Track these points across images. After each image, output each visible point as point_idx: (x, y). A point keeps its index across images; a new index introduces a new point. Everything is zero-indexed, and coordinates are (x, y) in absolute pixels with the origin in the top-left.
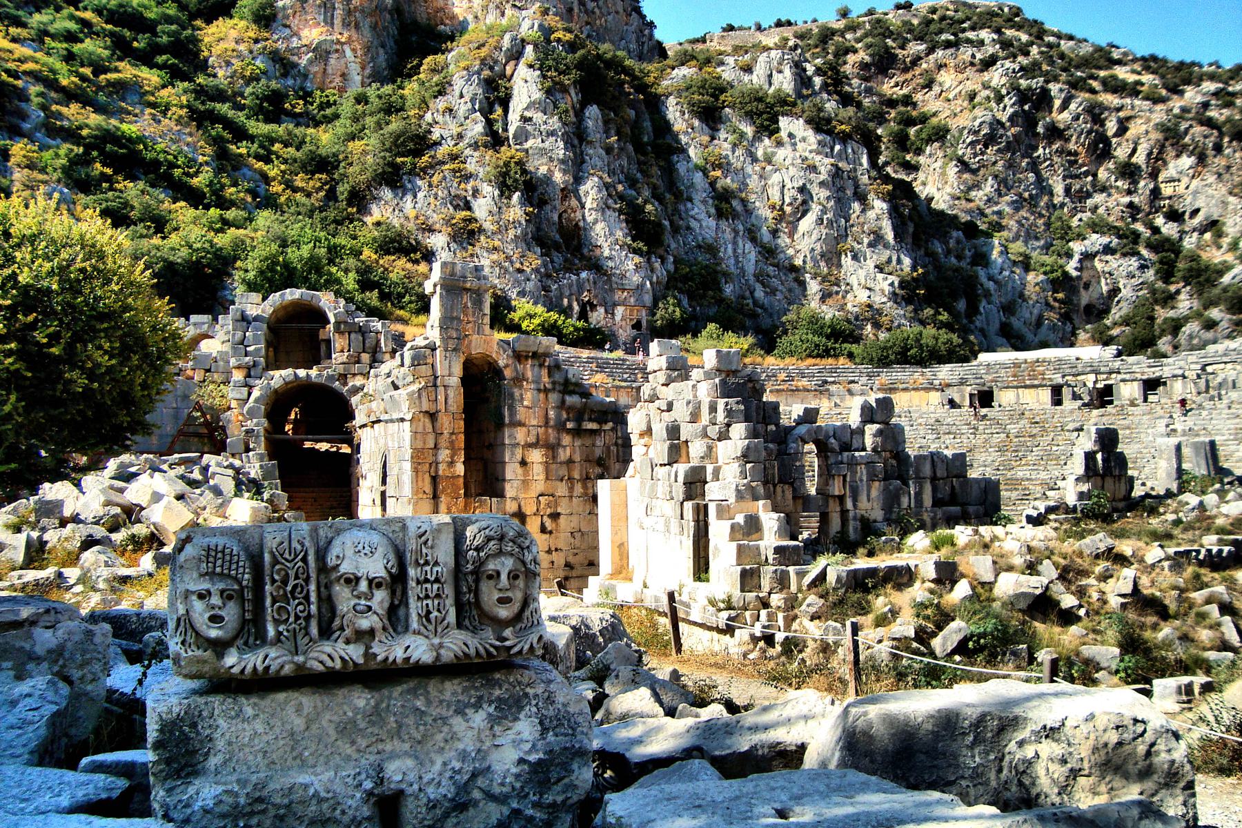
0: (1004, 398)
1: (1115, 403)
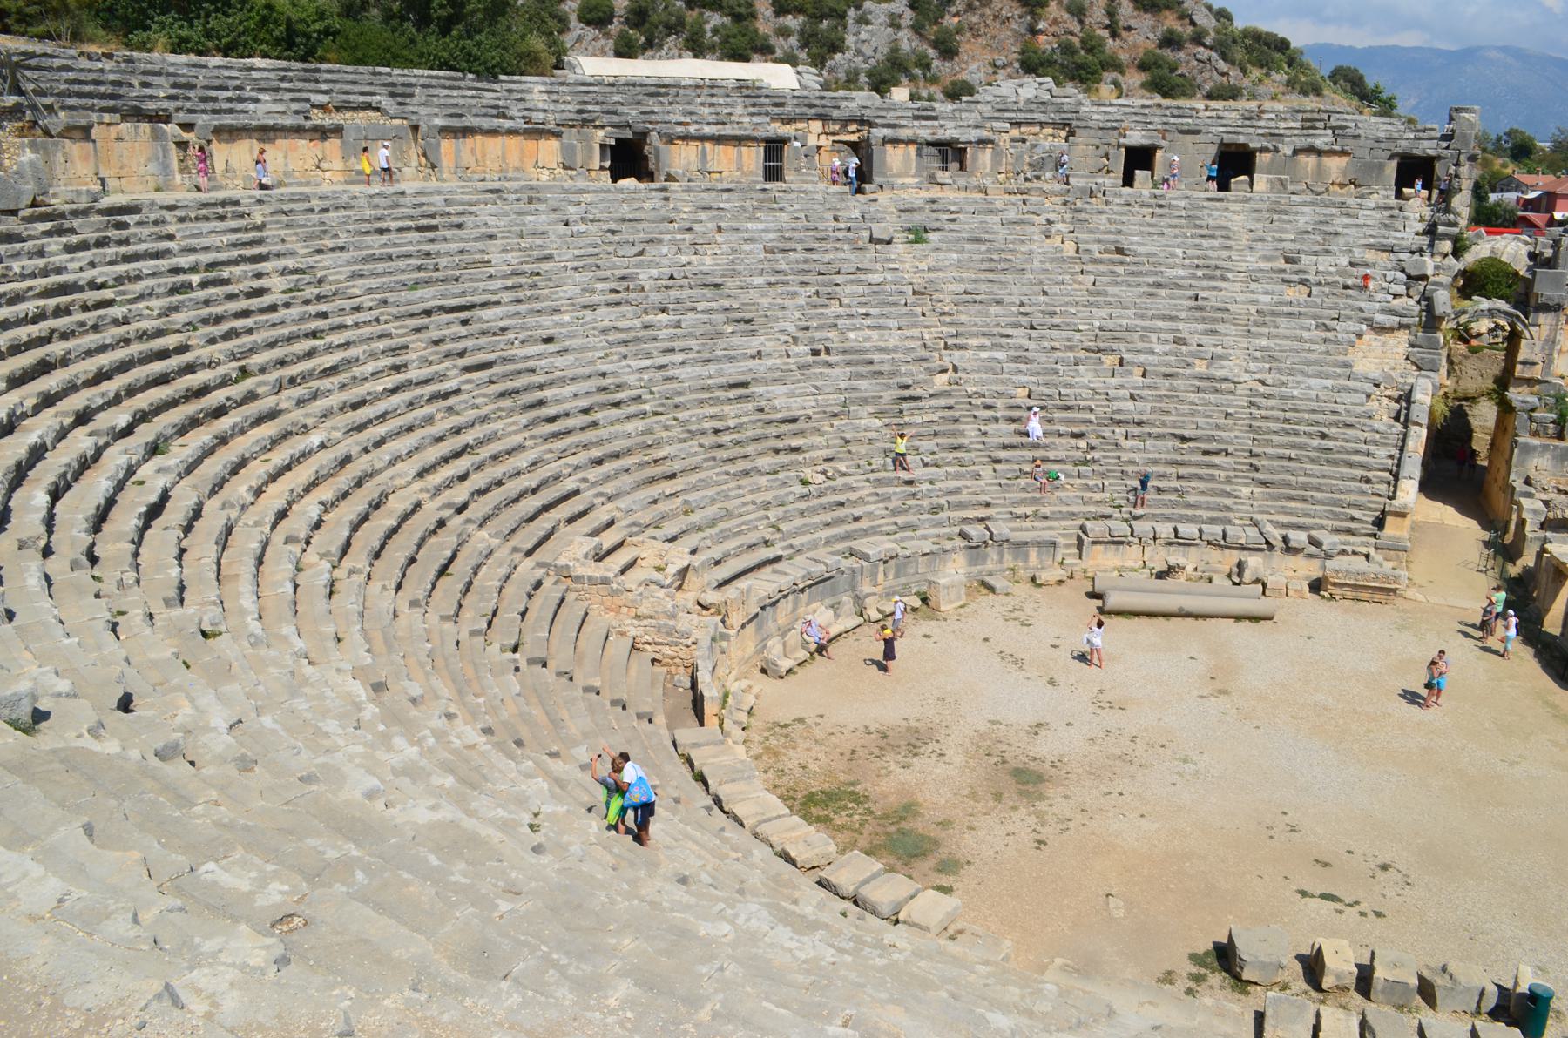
0: (681, 158)
1: (878, 179)
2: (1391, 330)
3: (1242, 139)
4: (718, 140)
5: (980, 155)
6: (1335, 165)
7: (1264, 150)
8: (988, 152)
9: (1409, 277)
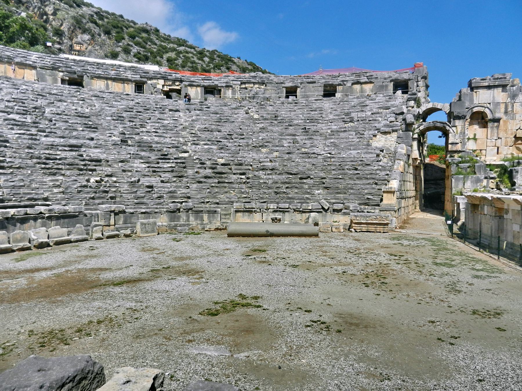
2: (390, 133)
3: (330, 83)
4: (114, 80)
5: (227, 91)
6: (368, 87)
7: (340, 85)
8: (230, 91)
9: (396, 114)
